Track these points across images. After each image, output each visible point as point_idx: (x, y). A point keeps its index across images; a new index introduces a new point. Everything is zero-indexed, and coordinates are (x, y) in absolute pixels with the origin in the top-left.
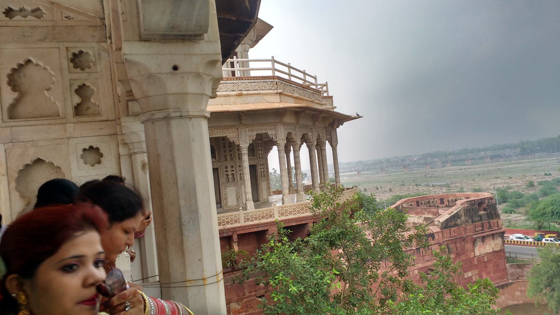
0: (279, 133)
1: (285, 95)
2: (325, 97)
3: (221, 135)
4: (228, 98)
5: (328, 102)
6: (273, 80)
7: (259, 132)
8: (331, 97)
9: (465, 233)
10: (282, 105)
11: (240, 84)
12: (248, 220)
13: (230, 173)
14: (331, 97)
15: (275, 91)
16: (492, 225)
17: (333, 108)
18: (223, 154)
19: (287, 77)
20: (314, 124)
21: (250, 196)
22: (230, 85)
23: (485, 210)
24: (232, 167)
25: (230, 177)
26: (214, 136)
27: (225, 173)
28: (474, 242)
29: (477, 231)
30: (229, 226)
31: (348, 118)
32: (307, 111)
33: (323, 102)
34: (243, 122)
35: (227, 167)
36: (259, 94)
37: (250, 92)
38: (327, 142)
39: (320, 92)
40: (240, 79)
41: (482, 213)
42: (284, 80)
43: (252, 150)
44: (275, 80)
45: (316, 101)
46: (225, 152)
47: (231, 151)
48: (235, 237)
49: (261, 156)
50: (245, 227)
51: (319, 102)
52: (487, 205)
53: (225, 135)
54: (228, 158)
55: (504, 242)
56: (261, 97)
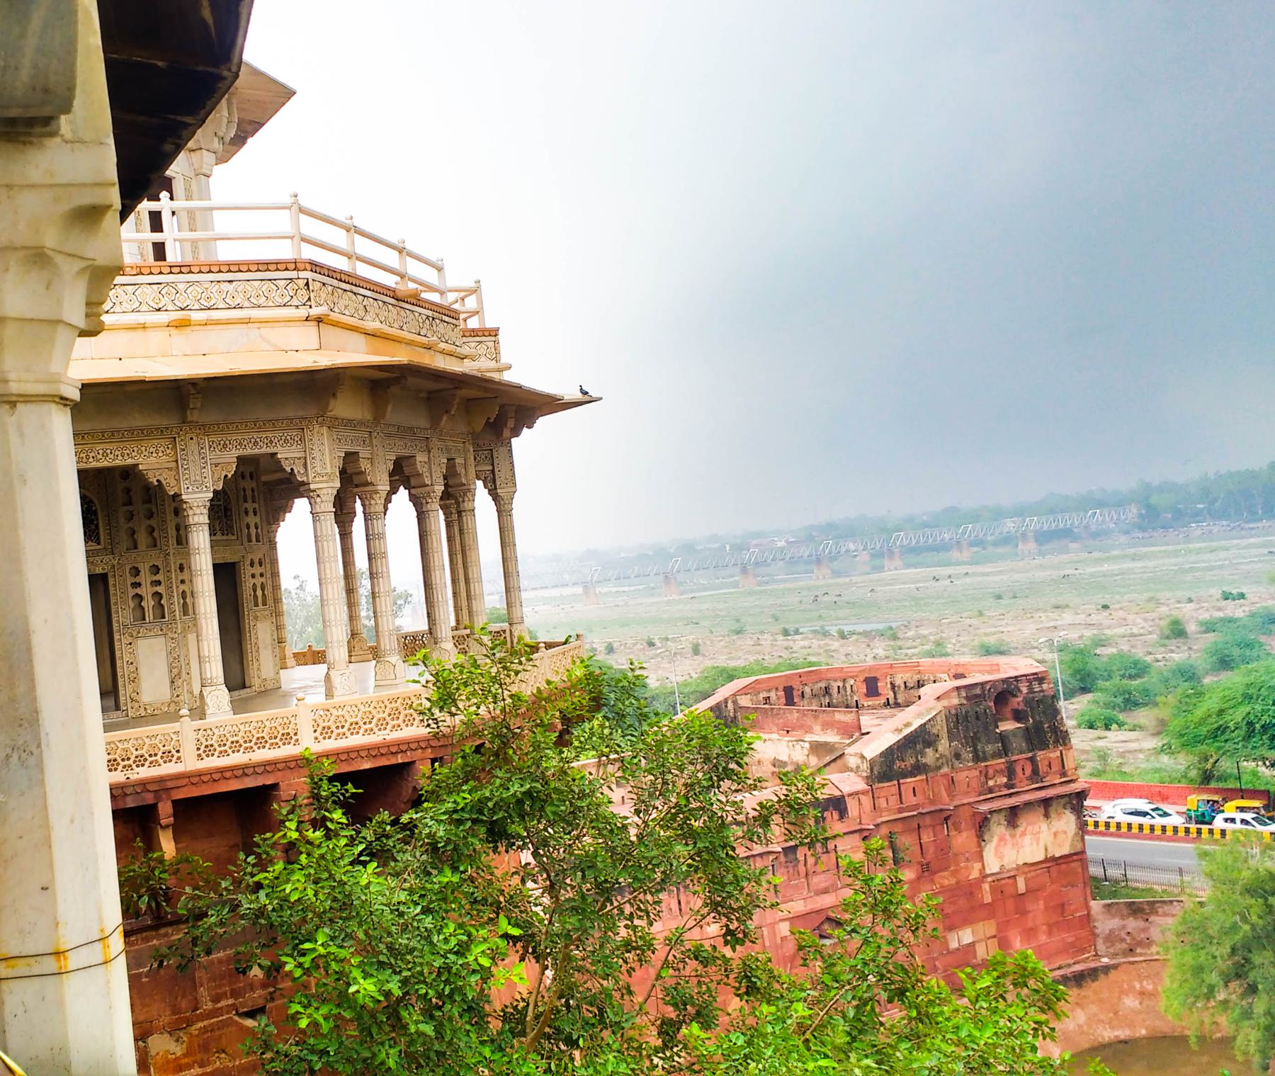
0: (316, 454)
1: (336, 324)
2: (474, 333)
3: (118, 462)
4: (139, 335)
5: (482, 349)
6: (293, 274)
7: (248, 452)
8: (494, 333)
9: (951, 796)
10: (324, 360)
11: (181, 287)
12: (209, 750)
13: (146, 591)
14: (494, 333)
15: (303, 312)
16: (1043, 768)
17: (500, 370)
18: (124, 525)
19: (340, 263)
20: (435, 423)
21: (215, 669)
22: (148, 289)
23: (1018, 716)
24: (155, 569)
25: (149, 603)
26: (94, 464)
27: (132, 592)
28: (982, 825)
29: (991, 790)
30: (144, 773)
31: (553, 404)
32: (411, 381)
33: (465, 350)
34: (193, 416)
35: (136, 572)
36: (248, 321)
37: (215, 315)
38: (480, 484)
39: (454, 315)
40: (182, 268)
41: (1007, 726)
42: (331, 272)
43: (223, 511)
44: (303, 274)
45: (443, 345)
46: (130, 517)
47: (150, 516)
48: (165, 810)
49: (253, 531)
50: (200, 774)
51: (452, 348)
52: (1027, 702)
53: (130, 461)
54: (142, 538)
55: (1082, 826)
56: (253, 332)
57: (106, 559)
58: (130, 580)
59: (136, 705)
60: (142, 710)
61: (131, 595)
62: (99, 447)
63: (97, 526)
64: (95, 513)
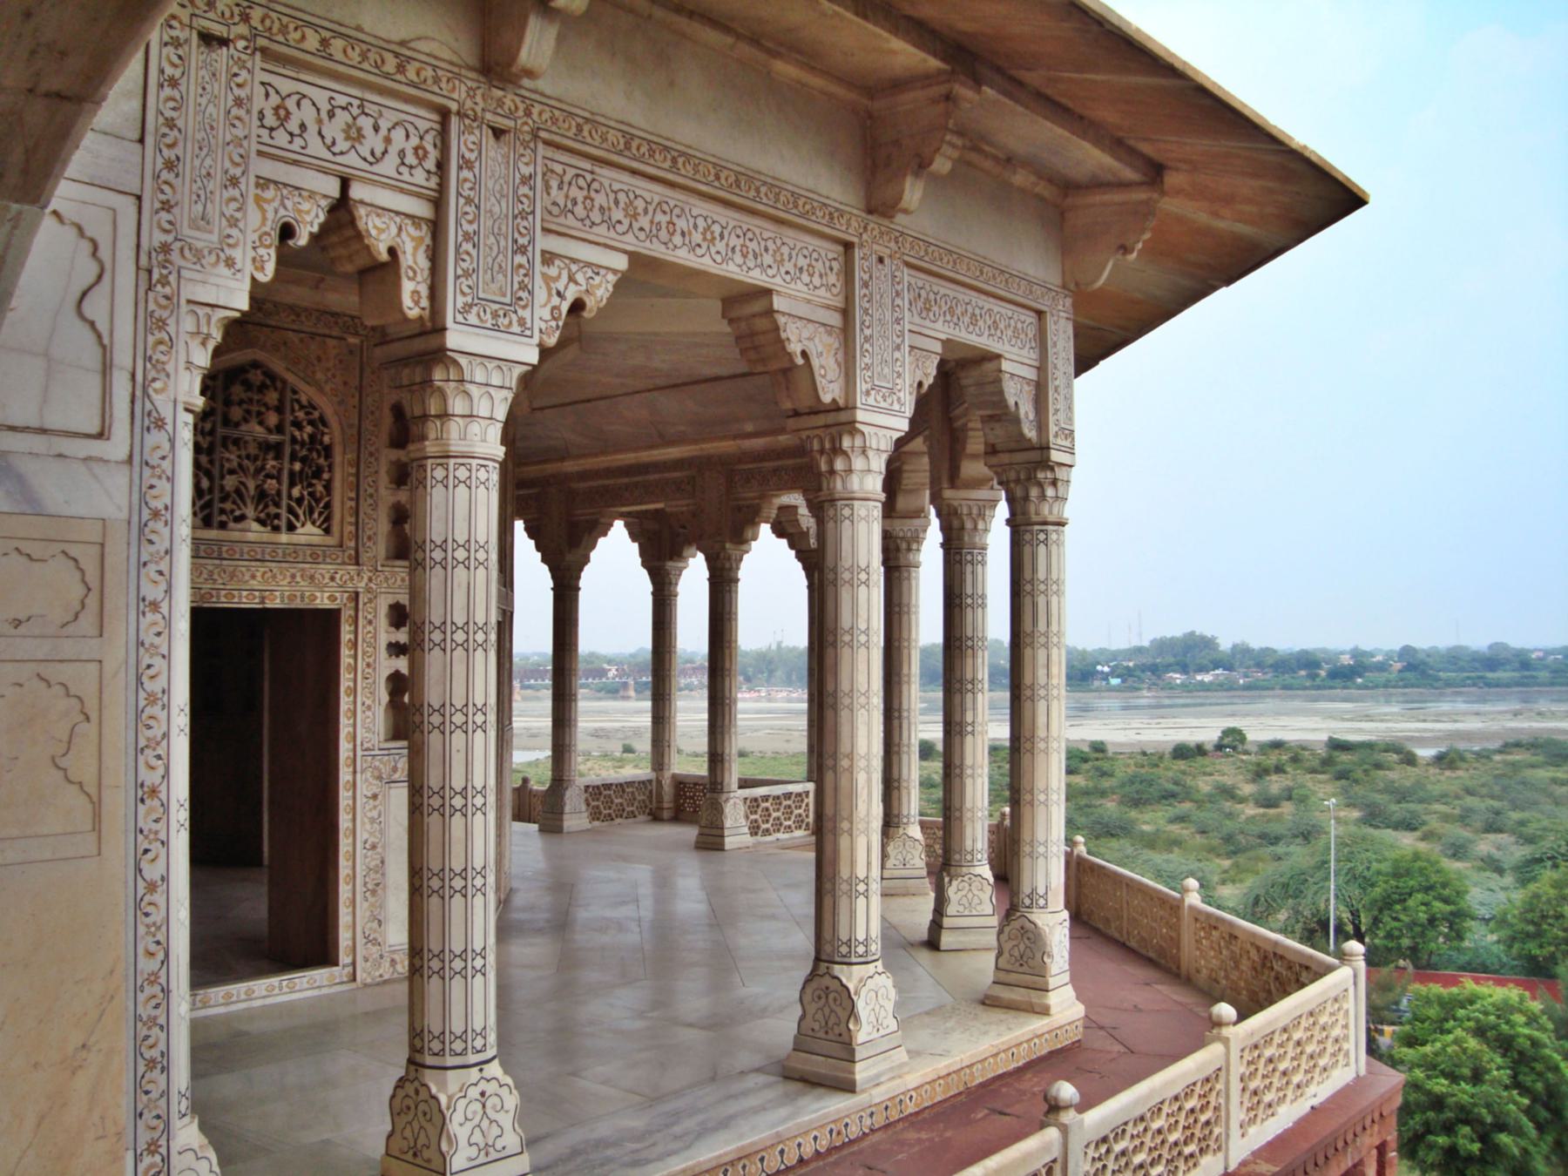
26: (683, 257)
27: (389, 665)
53: (757, 277)
58: (386, 634)
59: (375, 949)
60: (386, 964)
61: (386, 673)
62: (700, 207)
63: (328, 487)
64: (328, 451)
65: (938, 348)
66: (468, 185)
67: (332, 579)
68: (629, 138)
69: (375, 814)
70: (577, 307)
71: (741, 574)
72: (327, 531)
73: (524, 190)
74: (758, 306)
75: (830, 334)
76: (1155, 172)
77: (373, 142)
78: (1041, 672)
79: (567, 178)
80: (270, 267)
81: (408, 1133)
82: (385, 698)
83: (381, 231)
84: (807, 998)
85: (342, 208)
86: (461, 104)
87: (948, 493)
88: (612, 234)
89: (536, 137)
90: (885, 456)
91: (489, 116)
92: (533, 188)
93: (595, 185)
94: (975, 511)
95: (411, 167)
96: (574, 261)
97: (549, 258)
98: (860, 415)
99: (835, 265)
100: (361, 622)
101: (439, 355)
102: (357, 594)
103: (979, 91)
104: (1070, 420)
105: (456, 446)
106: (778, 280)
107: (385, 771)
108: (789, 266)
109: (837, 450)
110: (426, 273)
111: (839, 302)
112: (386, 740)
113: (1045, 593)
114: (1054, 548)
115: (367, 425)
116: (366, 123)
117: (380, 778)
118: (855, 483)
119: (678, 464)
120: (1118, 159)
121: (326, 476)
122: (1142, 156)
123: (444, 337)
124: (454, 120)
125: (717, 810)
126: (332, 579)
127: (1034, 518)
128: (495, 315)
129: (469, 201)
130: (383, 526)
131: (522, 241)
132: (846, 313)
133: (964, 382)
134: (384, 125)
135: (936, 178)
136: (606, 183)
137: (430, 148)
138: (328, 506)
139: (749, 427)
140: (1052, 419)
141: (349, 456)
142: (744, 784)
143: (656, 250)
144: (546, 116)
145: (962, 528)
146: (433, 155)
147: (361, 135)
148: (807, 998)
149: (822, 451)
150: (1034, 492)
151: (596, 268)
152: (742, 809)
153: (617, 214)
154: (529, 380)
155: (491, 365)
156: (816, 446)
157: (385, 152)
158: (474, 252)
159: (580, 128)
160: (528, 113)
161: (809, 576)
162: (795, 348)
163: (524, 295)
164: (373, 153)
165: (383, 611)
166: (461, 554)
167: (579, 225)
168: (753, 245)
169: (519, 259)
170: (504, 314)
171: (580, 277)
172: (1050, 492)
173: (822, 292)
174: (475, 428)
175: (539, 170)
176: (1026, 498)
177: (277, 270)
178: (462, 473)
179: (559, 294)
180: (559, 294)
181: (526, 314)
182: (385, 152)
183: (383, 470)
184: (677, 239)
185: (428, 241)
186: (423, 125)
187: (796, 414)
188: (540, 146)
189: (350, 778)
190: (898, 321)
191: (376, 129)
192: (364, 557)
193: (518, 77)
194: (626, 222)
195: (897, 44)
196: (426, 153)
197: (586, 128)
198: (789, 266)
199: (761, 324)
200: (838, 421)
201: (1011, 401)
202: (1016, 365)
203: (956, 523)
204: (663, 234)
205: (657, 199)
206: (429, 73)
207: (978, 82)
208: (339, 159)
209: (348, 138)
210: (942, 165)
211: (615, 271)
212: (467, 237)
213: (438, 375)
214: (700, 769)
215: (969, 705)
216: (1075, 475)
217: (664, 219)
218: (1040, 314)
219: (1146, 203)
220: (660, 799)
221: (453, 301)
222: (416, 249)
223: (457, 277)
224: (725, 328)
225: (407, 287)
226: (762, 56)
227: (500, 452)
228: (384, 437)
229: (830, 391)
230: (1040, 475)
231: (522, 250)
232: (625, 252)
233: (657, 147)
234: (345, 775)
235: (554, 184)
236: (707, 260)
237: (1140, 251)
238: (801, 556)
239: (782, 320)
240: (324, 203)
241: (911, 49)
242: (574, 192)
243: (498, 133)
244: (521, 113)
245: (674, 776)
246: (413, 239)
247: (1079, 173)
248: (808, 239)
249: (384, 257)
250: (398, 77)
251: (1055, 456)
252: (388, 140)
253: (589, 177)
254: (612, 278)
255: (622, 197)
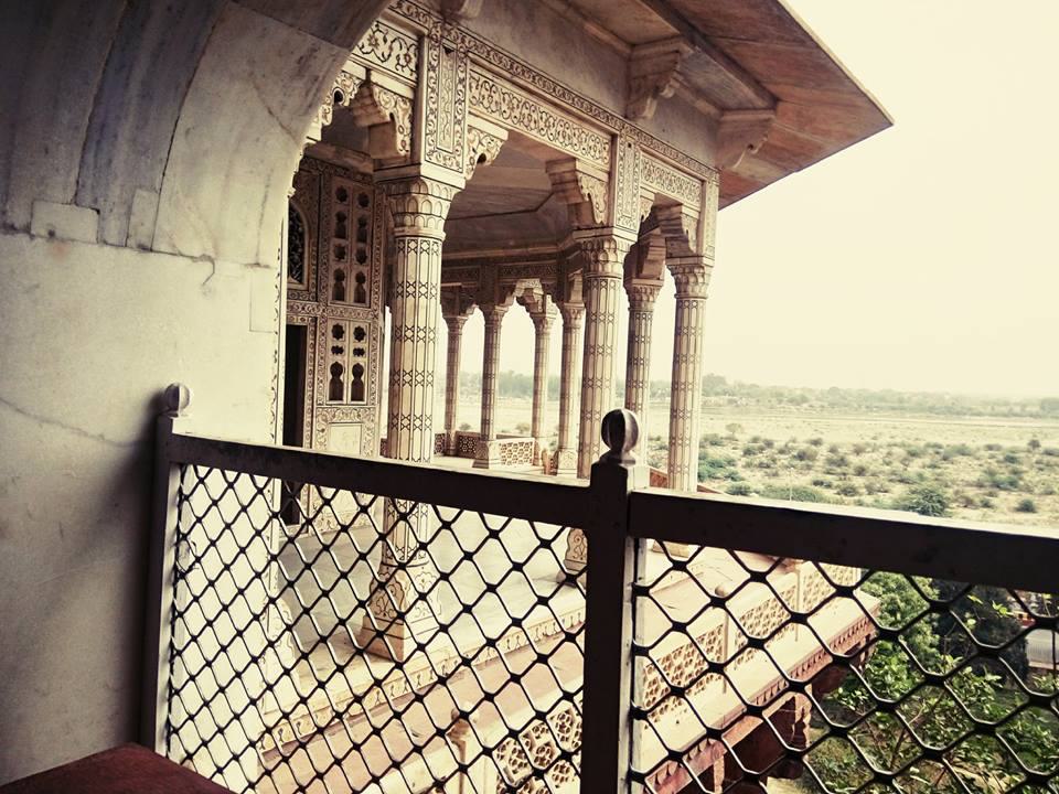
24: (359, 334)
25: (347, 378)
26: (534, 135)
27: (332, 359)
35: (338, 332)
46: (341, 254)
53: (569, 150)
54: (350, 285)
57: (311, 305)
58: (332, 342)
64: (301, 236)
65: (652, 197)
66: (433, 81)
67: (303, 309)
68: (513, 62)
69: (322, 440)
70: (482, 159)
71: (502, 323)
72: (301, 282)
73: (460, 87)
74: (567, 167)
75: (602, 185)
76: (775, 101)
77: (383, 48)
78: (690, 376)
79: (480, 83)
80: (330, 117)
81: (381, 603)
82: (330, 377)
83: (387, 103)
84: (571, 540)
85: (367, 84)
86: (430, 31)
87: (635, 281)
88: (501, 118)
89: (466, 56)
90: (625, 254)
91: (444, 41)
92: (464, 87)
93: (494, 89)
94: (649, 291)
95: (403, 67)
96: (482, 132)
97: (471, 128)
98: (615, 231)
99: (607, 146)
100: (318, 334)
101: (417, 178)
102: (316, 318)
103: (693, 49)
104: (713, 241)
105: (424, 231)
106: (578, 153)
107: (329, 417)
108: (584, 145)
109: (600, 249)
110: (409, 131)
111: (607, 168)
112: (331, 399)
113: (695, 334)
114: (700, 310)
115: (323, 223)
116: (379, 36)
117: (326, 421)
118: (609, 268)
119: (472, 261)
120: (757, 94)
121: (300, 250)
122: (769, 92)
123: (419, 168)
124: (426, 40)
125: (485, 449)
126: (303, 309)
127: (691, 294)
128: (445, 159)
129: (433, 91)
130: (332, 282)
131: (459, 117)
132: (610, 174)
133: (660, 218)
134: (390, 39)
135: (665, 104)
136: (499, 87)
137: (412, 56)
138: (301, 267)
139: (512, 243)
140: (705, 240)
141: (312, 240)
142: (499, 437)
143: (521, 129)
144: (472, 44)
145: (641, 300)
146: (414, 60)
147: (377, 45)
148: (571, 540)
149: (592, 250)
150: (692, 280)
151: (493, 137)
152: (498, 449)
153: (504, 107)
154: (462, 194)
155: (442, 186)
156: (589, 246)
157: (389, 55)
158: (435, 121)
159: (488, 52)
160: (463, 41)
161: (537, 327)
162: (585, 191)
163: (459, 149)
164: (383, 55)
165: (330, 328)
166: (423, 290)
167: (485, 111)
168: (568, 132)
169: (457, 128)
170: (448, 158)
171: (484, 142)
172: (700, 280)
173: (600, 161)
174: (432, 222)
175: (468, 76)
176: (687, 283)
177: (333, 119)
178: (425, 246)
179: (474, 150)
180: (474, 150)
181: (459, 159)
182: (389, 55)
183: (332, 248)
184: (532, 125)
185: (410, 112)
186: (410, 42)
187: (579, 229)
188: (469, 66)
189: (309, 420)
190: (636, 180)
191: (385, 41)
192: (321, 298)
193: (461, 17)
194: (508, 112)
195: (656, 17)
196: (410, 59)
197: (492, 53)
198: (584, 145)
199: (568, 176)
200: (604, 232)
201: (685, 229)
202: (689, 210)
203: (638, 298)
204: (526, 120)
205: (524, 100)
206: (413, 10)
207: (693, 42)
208: (366, 56)
209: (370, 45)
210: (668, 93)
211: (502, 140)
212: (432, 112)
213: (414, 189)
214: (476, 428)
215: (640, 394)
216: (713, 272)
217: (526, 112)
218: (703, 181)
219: (768, 120)
220: (449, 445)
221: (425, 148)
222: (404, 115)
223: (427, 135)
224: (546, 175)
225: (400, 137)
226: (580, 19)
227: (443, 235)
228: (333, 232)
229: (600, 218)
230: (696, 271)
231: (459, 122)
232: (506, 129)
233: (526, 70)
234: (307, 419)
235: (474, 85)
236: (546, 138)
237: (760, 150)
238: (533, 316)
239: (580, 175)
240: (357, 82)
241: (660, 19)
242: (484, 92)
243: (448, 51)
244: (459, 41)
245: (457, 432)
246: (403, 110)
247: (731, 103)
248: (595, 131)
249: (388, 119)
250: (398, 10)
251: (705, 261)
252: (391, 48)
253: (491, 83)
254: (500, 144)
255: (506, 96)
